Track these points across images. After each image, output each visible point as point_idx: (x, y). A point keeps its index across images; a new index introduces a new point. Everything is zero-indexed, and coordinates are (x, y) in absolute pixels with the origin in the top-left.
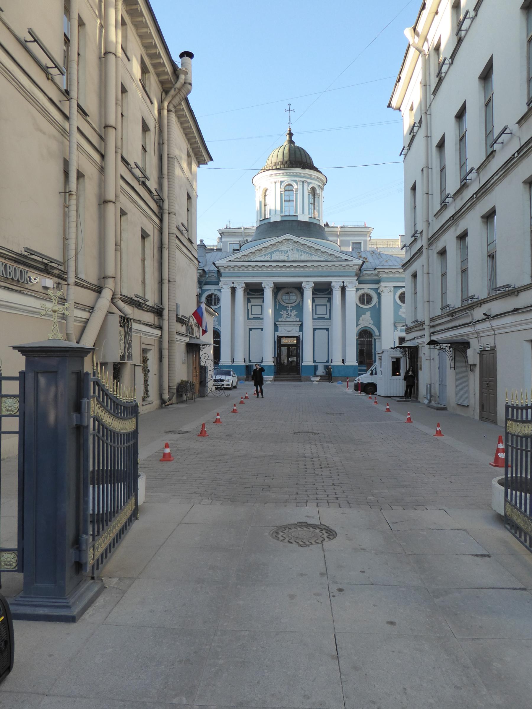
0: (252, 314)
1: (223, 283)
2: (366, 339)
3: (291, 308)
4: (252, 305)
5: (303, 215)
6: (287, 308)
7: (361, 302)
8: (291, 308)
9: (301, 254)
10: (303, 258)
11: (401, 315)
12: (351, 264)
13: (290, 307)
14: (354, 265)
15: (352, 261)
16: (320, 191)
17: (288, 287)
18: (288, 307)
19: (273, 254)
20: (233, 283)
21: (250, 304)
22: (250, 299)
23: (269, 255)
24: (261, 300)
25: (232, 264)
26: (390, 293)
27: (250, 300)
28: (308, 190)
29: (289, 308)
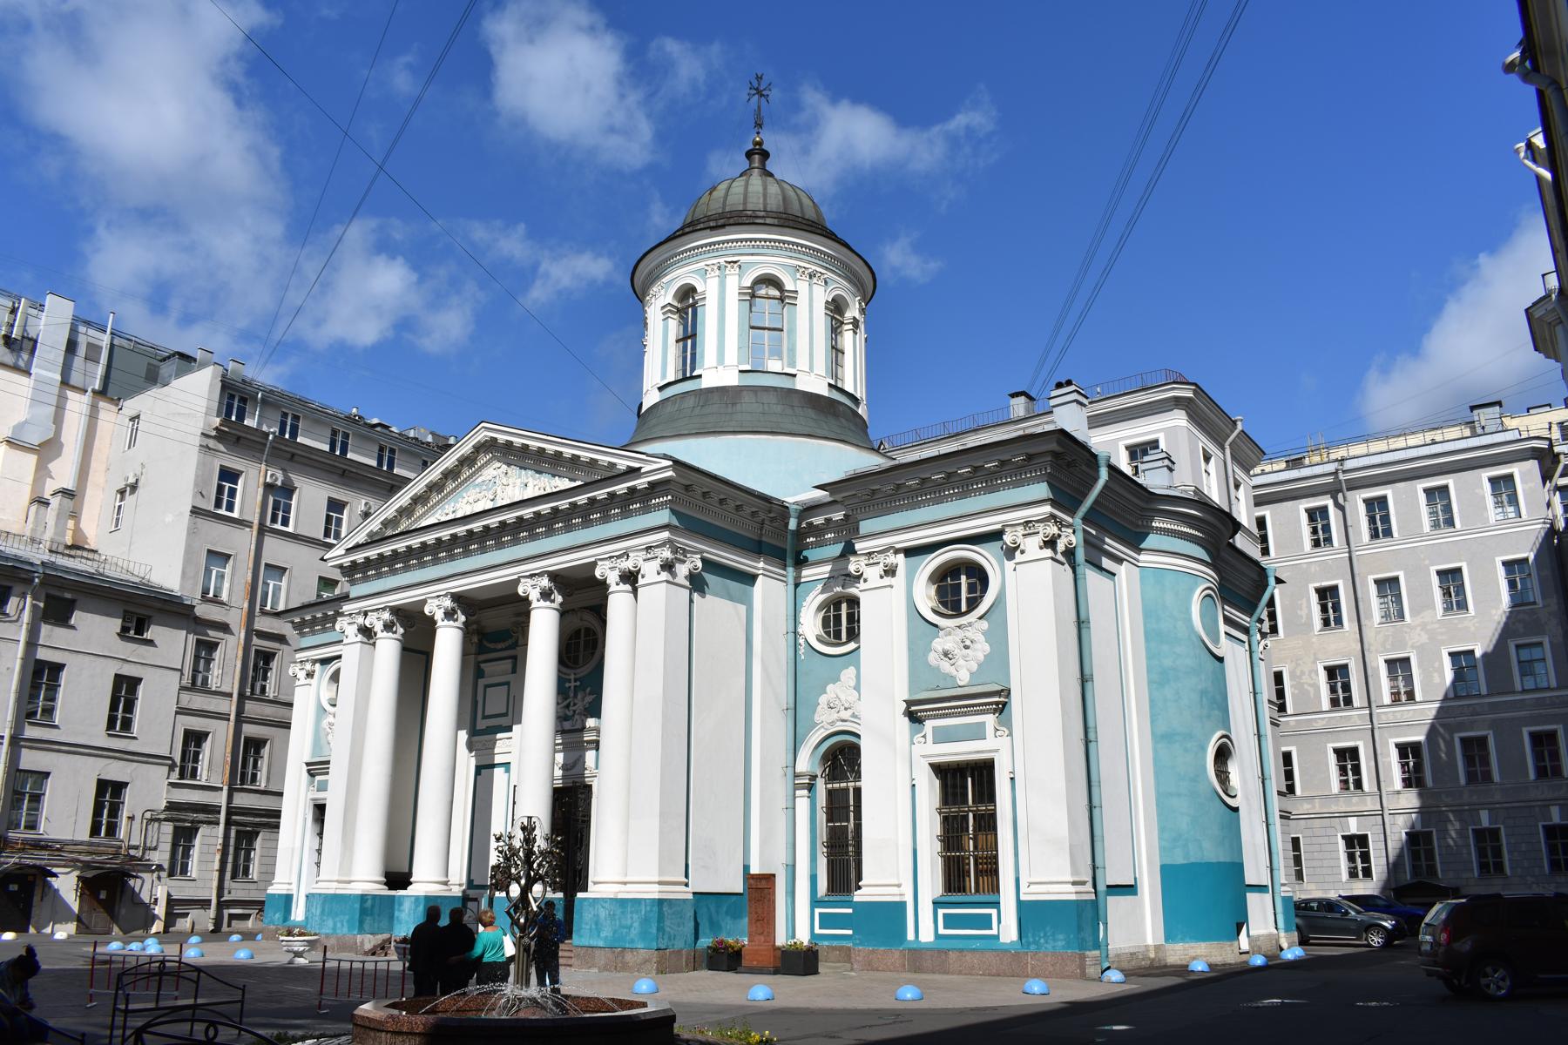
0: (485, 717)
1: (345, 618)
2: (853, 784)
3: (578, 683)
4: (487, 686)
5: (720, 368)
6: (567, 685)
7: (828, 633)
8: (578, 683)
9: (526, 481)
10: (530, 493)
11: (938, 668)
12: (641, 483)
13: (575, 681)
14: (652, 485)
15: (640, 468)
16: (802, 287)
17: (573, 610)
18: (570, 681)
19: (460, 500)
20: (366, 614)
21: (482, 682)
22: (482, 665)
23: (452, 504)
24: (507, 664)
25: (359, 557)
26: (887, 580)
27: (483, 671)
28: (741, 288)
29: (573, 684)
